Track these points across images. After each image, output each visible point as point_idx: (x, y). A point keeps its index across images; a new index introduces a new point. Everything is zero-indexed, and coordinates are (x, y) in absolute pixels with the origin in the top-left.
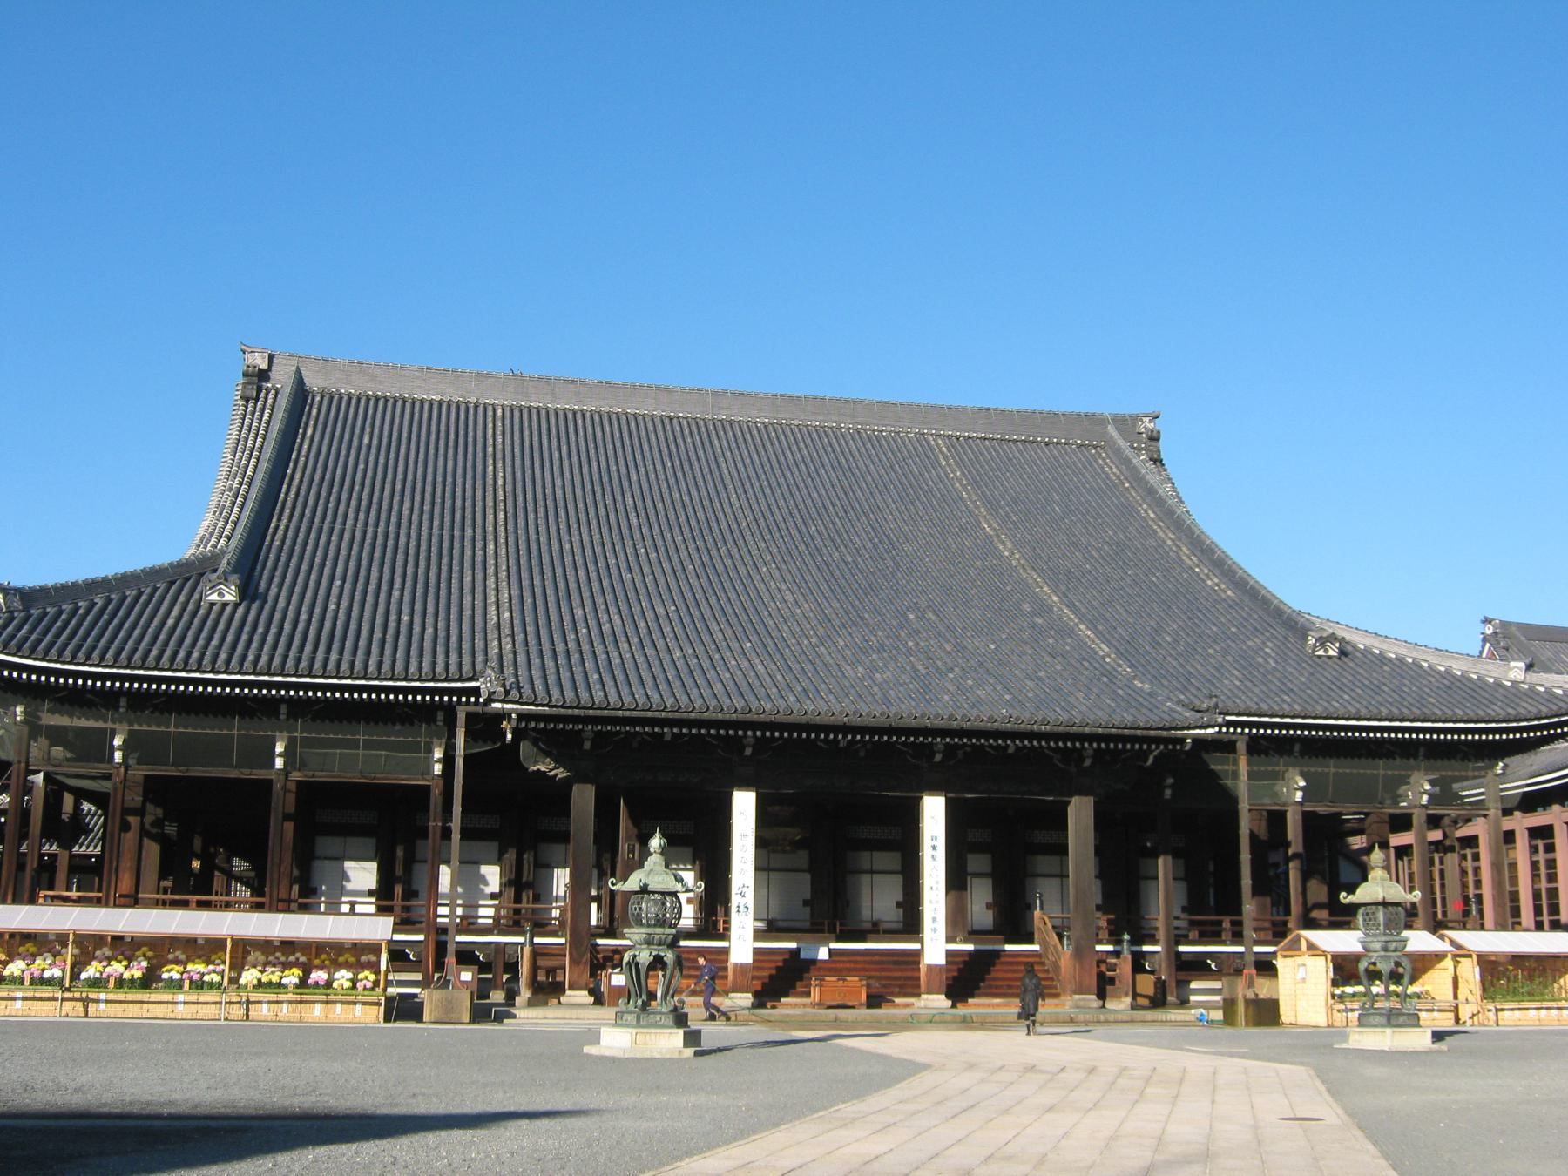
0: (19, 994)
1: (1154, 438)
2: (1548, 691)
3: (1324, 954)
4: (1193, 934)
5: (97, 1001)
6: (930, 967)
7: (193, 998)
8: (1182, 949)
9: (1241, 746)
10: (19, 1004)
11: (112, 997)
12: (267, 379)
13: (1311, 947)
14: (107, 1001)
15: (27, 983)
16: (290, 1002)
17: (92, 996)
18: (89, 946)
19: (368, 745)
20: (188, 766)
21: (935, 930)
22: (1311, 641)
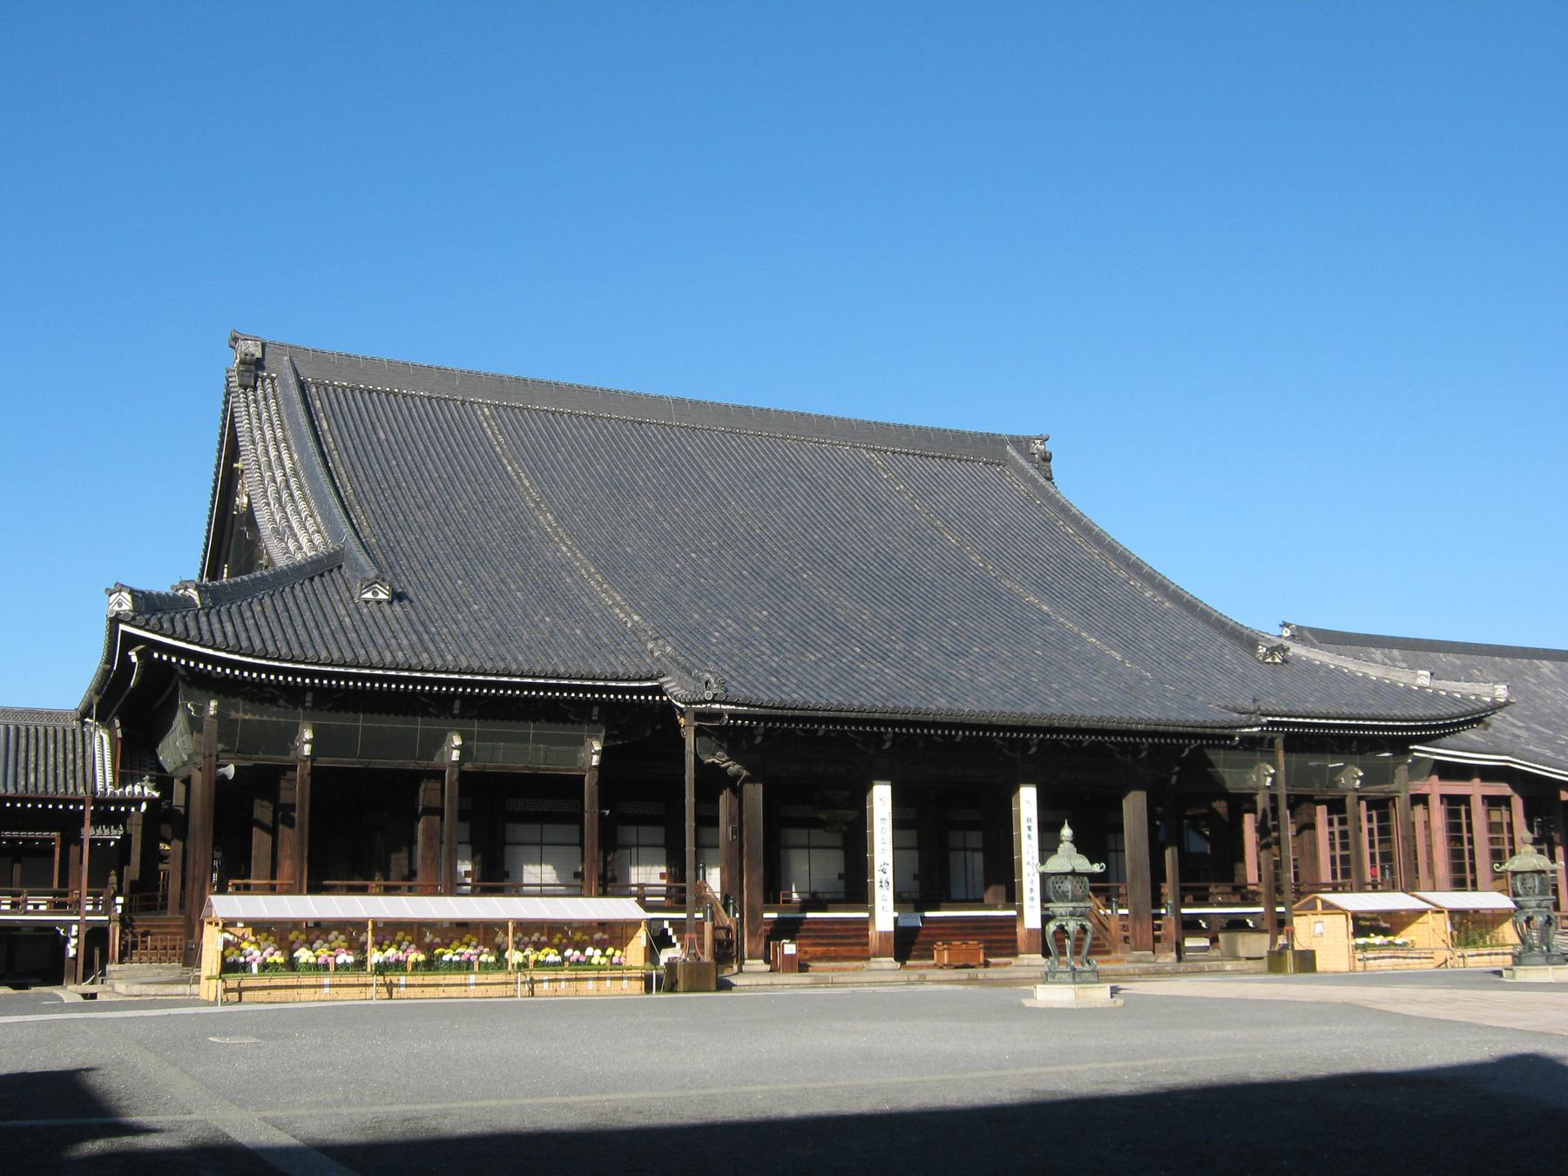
0: (327, 981)
1: (1047, 458)
2: (1449, 695)
3: (1344, 912)
4: (1189, 899)
5: (398, 986)
6: (1030, 931)
7: (482, 978)
8: (1184, 911)
9: (1279, 742)
10: (327, 990)
11: (411, 980)
12: (263, 368)
13: (1329, 908)
14: (407, 986)
15: (332, 968)
16: (568, 980)
17: (395, 980)
18: (389, 931)
19: (538, 739)
20: (303, 757)
21: (1032, 899)
22: (1262, 650)
